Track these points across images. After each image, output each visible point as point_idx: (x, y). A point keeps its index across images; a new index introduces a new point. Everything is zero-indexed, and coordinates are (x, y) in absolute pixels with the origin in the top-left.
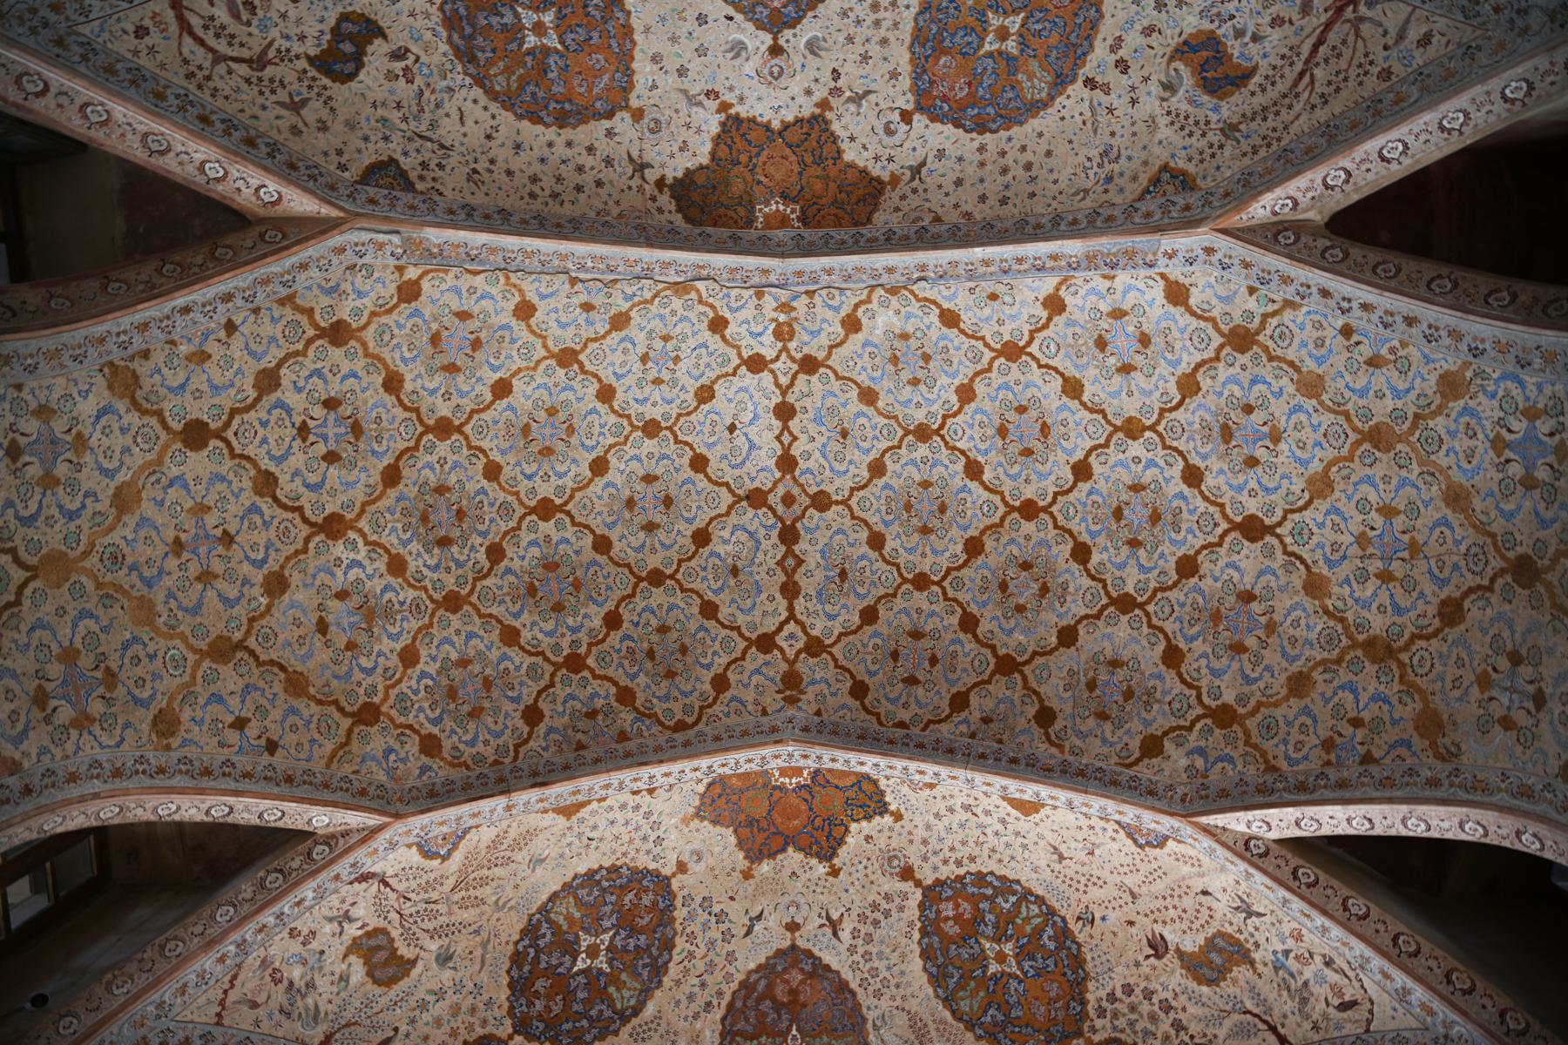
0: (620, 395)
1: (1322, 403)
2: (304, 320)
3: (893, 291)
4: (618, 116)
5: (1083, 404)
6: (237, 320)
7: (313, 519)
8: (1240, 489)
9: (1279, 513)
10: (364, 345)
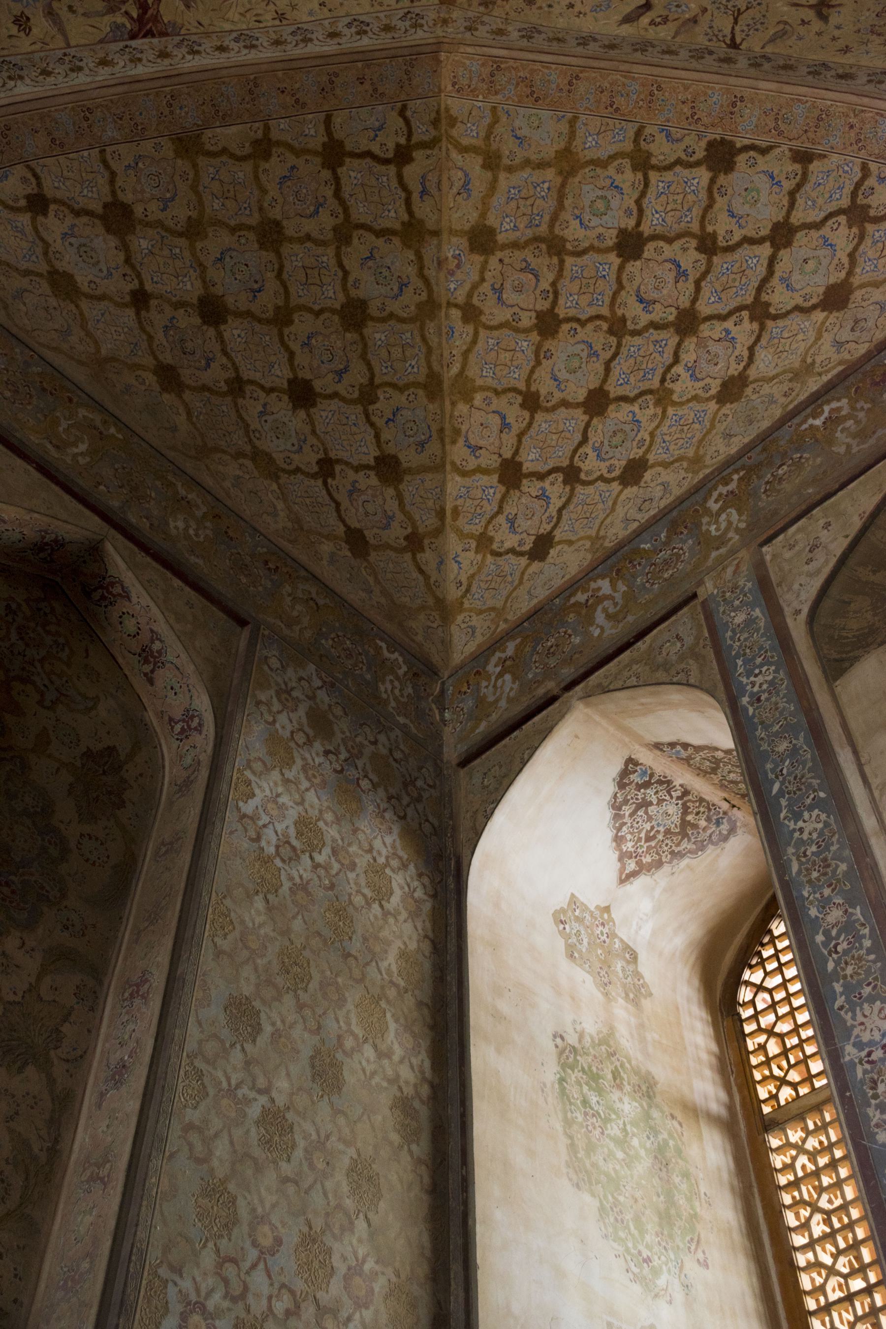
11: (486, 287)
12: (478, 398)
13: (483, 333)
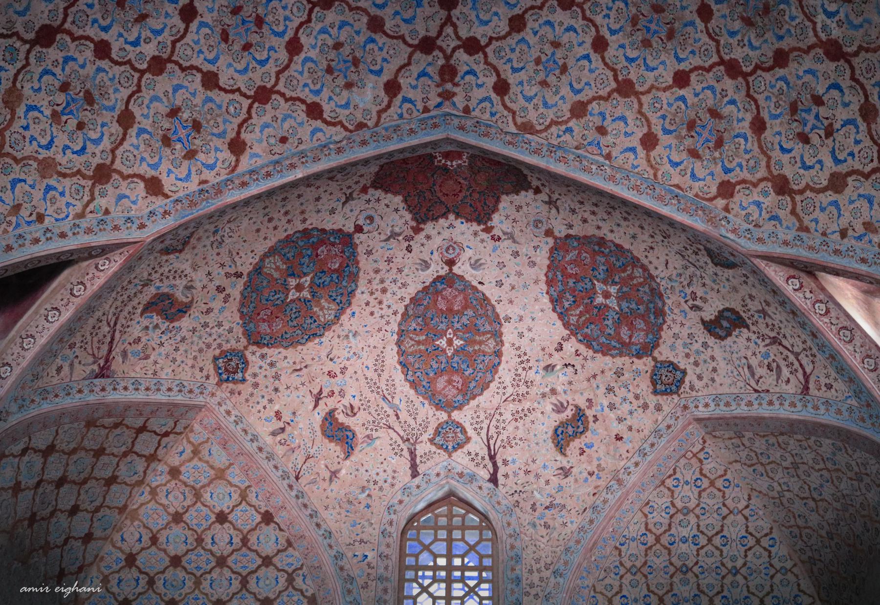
0: (589, 40)
1: (36, 159)
2: (799, 209)
3: (361, 126)
4: (563, 235)
5: (199, 70)
6: (837, 236)
7: (846, 66)
8: (67, 60)
9: (32, 60)
10: (768, 166)
11: (165, 488)
12: (136, 523)
13: (153, 502)
